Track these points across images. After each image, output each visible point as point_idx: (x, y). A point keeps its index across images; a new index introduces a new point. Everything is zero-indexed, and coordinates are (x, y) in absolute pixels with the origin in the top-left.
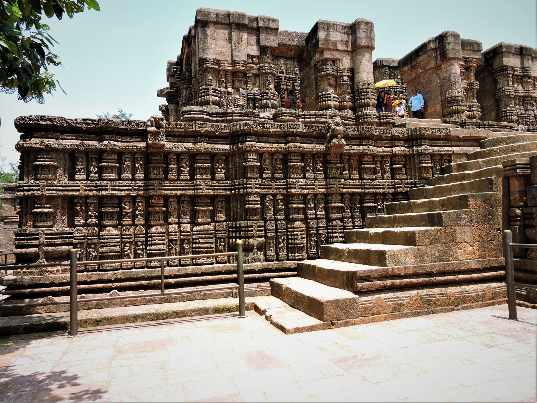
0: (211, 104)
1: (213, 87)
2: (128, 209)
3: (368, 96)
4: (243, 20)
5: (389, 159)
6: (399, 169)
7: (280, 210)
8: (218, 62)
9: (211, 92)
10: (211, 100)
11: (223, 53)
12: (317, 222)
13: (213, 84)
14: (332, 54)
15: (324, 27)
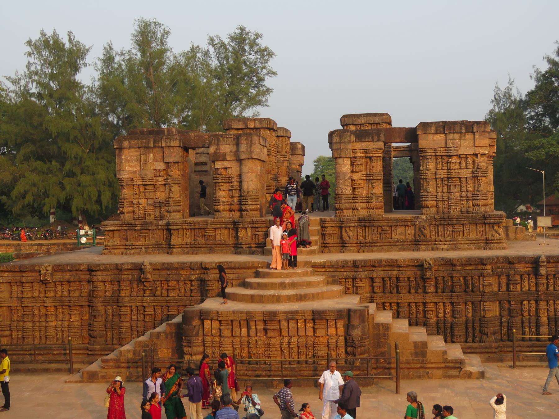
0: (125, 214)
1: (127, 200)
2: (36, 312)
3: (246, 203)
4: (148, 144)
5: (189, 282)
6: (194, 289)
7: (115, 316)
8: (132, 179)
9: (126, 205)
10: (125, 211)
11: (134, 172)
12: (137, 323)
13: (127, 198)
14: (223, 165)
15: (214, 142)
